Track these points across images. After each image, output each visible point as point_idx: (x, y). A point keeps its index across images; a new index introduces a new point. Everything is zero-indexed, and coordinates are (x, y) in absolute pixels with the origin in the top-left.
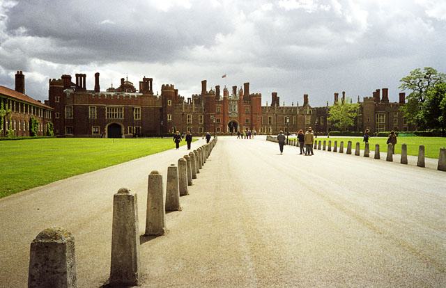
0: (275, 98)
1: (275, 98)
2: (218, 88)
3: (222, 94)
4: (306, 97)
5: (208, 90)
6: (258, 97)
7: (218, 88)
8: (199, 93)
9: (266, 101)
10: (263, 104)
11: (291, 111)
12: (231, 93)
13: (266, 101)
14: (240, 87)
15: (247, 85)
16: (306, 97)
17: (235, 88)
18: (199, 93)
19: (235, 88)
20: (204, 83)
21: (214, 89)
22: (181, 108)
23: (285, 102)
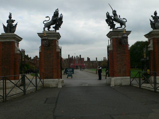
0: (88, 59)
1: (88, 59)
2: (72, 56)
3: (74, 58)
4: (96, 58)
5: (70, 57)
6: (83, 59)
7: (72, 56)
8: (68, 58)
9: (86, 59)
10: (85, 60)
11: (93, 62)
12: (76, 58)
13: (86, 59)
14: (79, 56)
15: (80, 56)
16: (96, 58)
17: (77, 56)
18: (68, 58)
19: (77, 56)
20: (69, 55)
21: (72, 57)
22: (63, 62)
23: (91, 60)
